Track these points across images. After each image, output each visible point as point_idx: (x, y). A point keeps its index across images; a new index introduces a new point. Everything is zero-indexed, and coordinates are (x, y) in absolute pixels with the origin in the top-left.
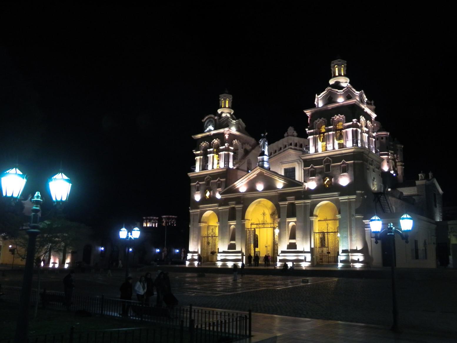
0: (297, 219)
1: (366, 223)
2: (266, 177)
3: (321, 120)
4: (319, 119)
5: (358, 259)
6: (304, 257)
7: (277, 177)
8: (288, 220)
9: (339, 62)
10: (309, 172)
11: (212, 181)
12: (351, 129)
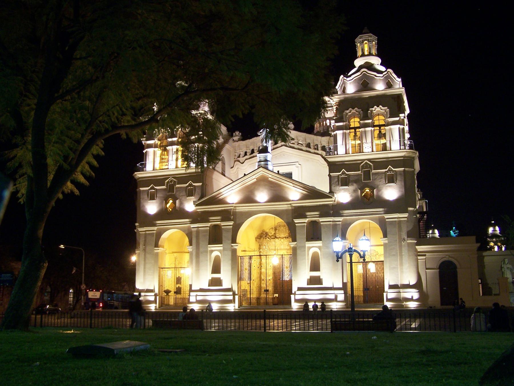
0: (322, 243)
1: (418, 250)
2: (271, 183)
3: (353, 111)
4: (350, 109)
5: (412, 297)
6: (334, 295)
7: (291, 184)
8: (309, 244)
9: (370, 37)
10: (338, 179)
11: (177, 186)
12: (398, 126)
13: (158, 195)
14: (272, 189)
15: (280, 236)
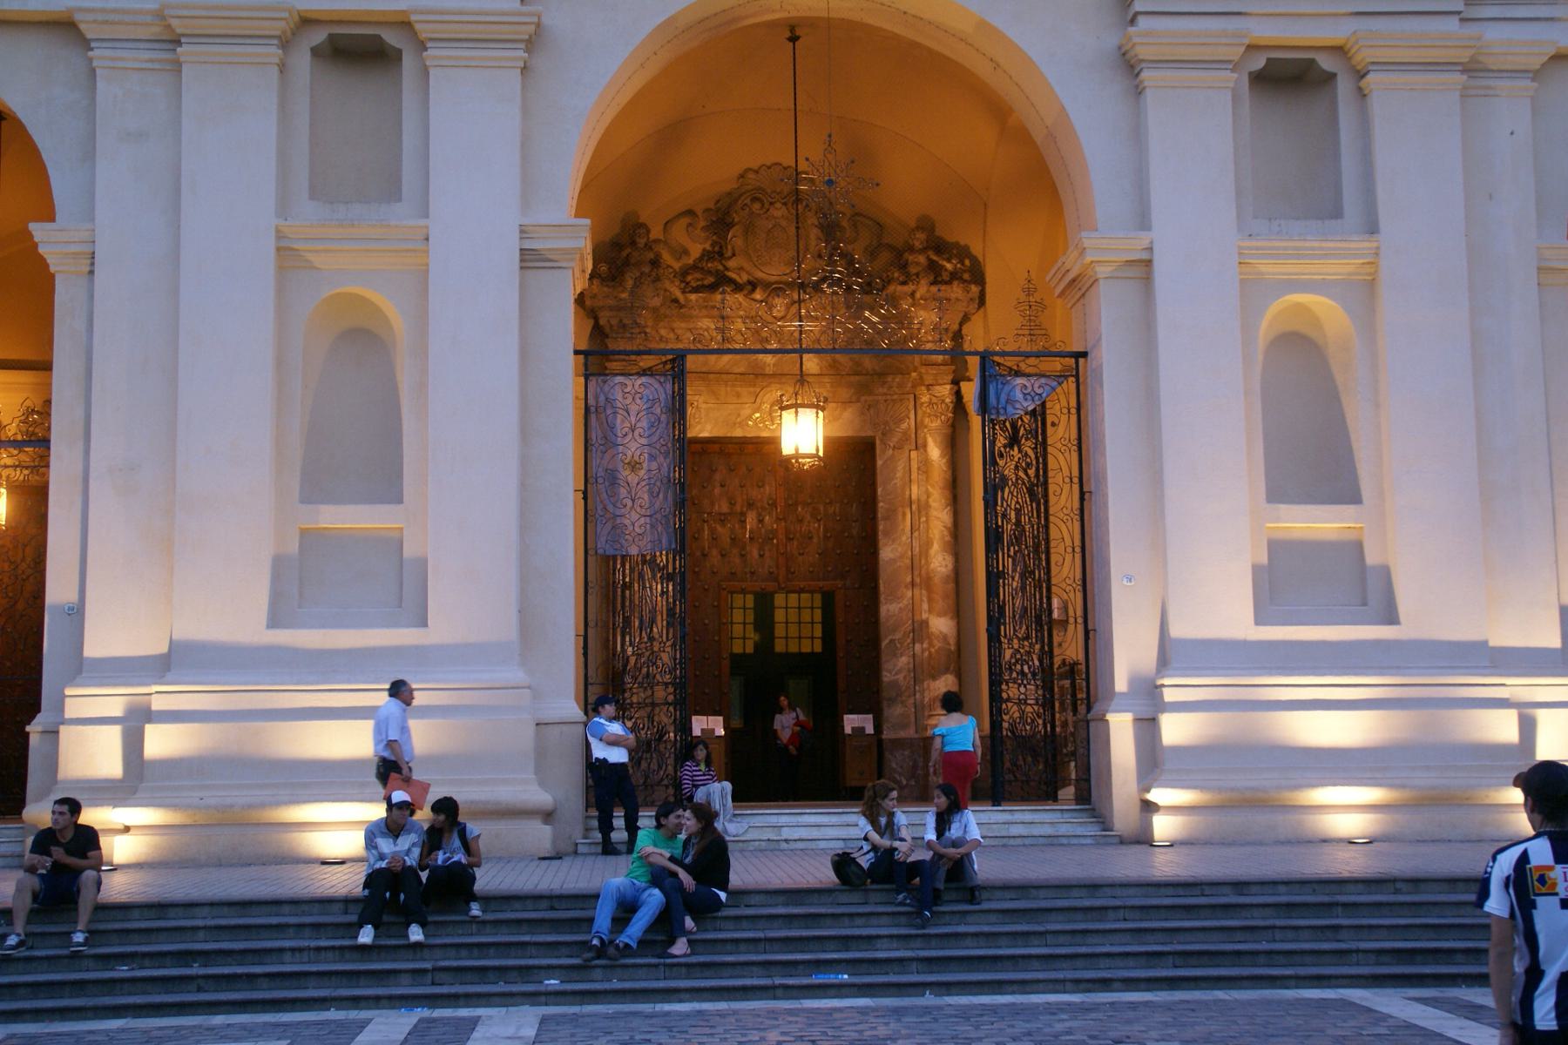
15: (760, 275)
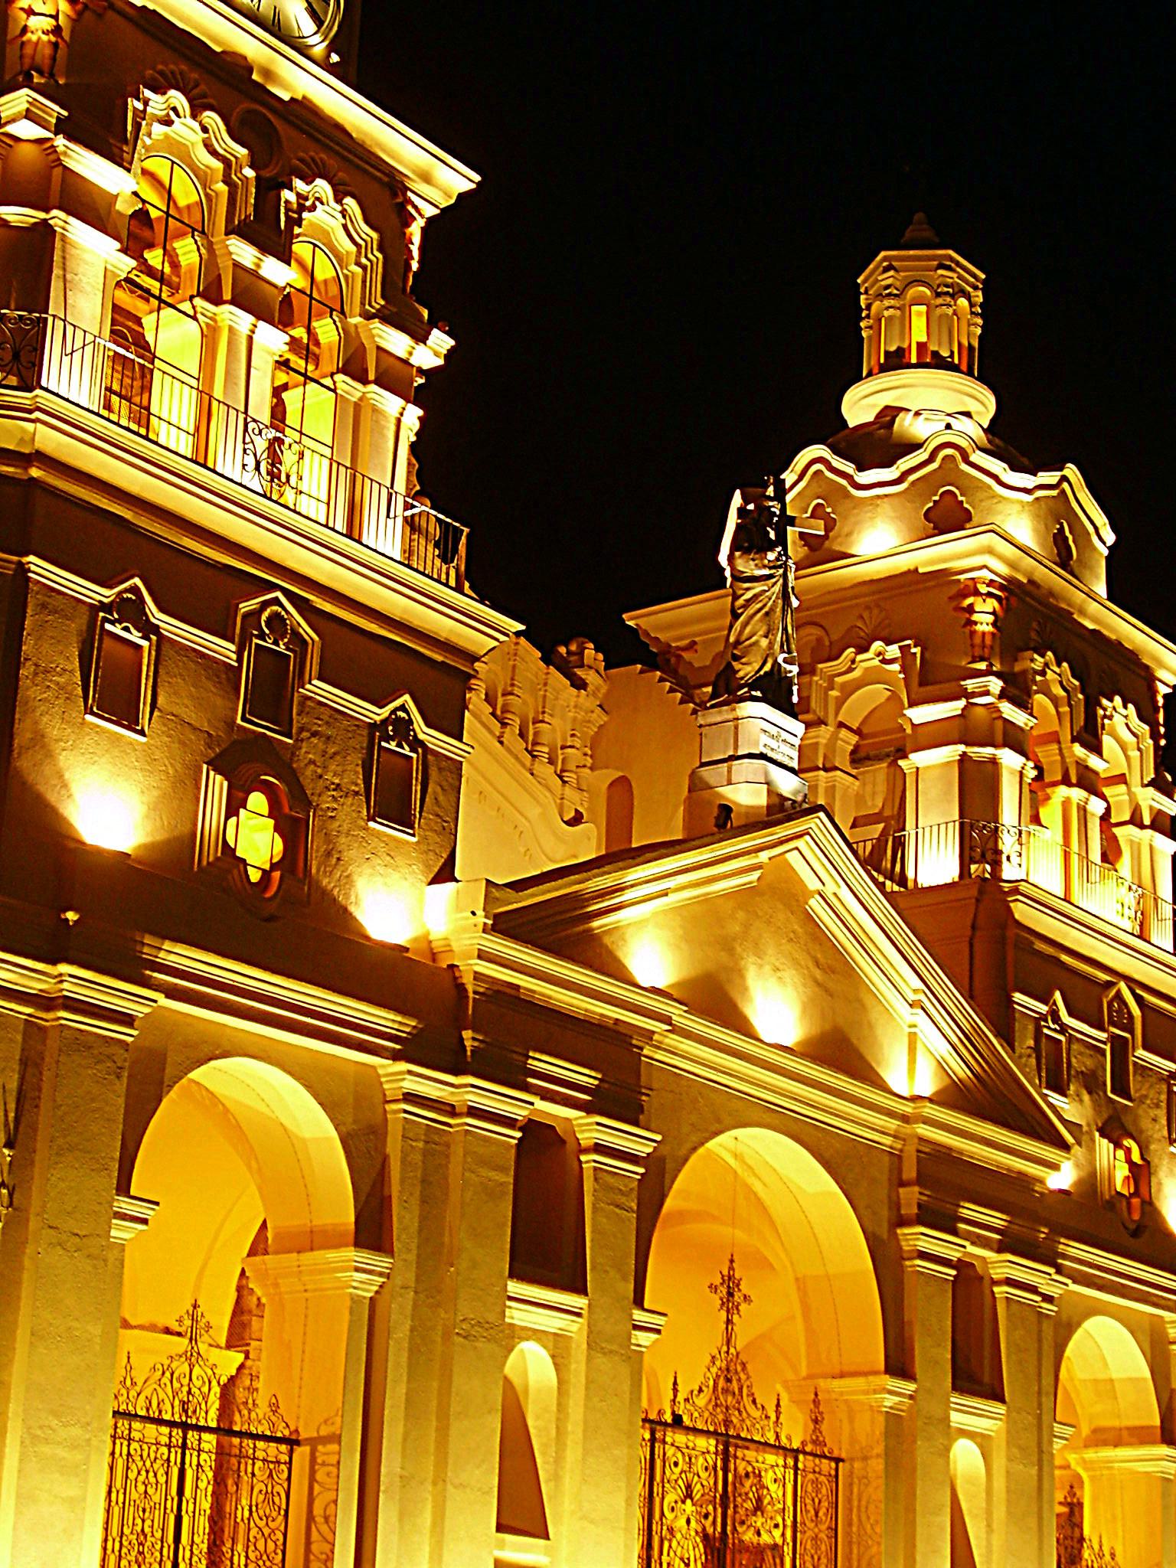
11: (319, 689)
13: (161, 700)
14: (818, 974)
